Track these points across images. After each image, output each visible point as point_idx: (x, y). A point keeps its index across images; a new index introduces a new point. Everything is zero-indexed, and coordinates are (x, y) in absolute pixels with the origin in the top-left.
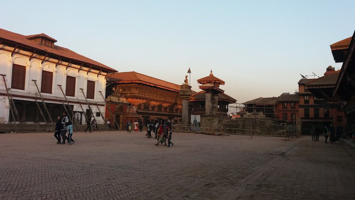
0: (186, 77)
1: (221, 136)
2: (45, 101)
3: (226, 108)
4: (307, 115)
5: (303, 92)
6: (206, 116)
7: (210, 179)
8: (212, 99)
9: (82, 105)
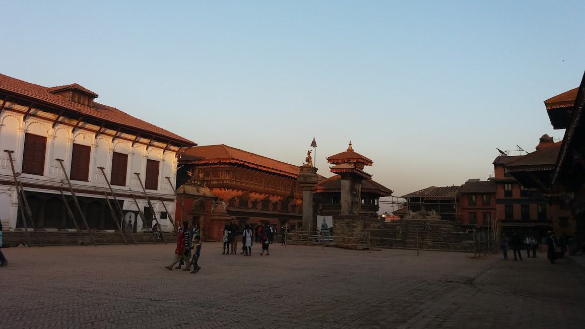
0: (309, 153)
1: (369, 251)
2: (77, 194)
3: (376, 204)
4: (509, 216)
5: (502, 177)
6: (342, 218)
7: (349, 325)
8: (352, 189)
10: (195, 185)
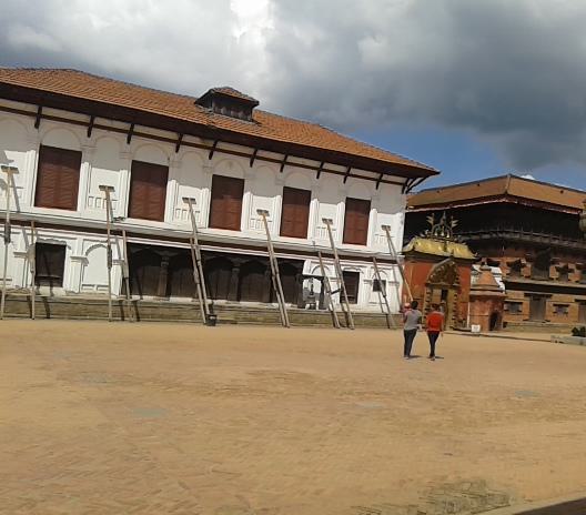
9: (325, 260)
10: (439, 238)
